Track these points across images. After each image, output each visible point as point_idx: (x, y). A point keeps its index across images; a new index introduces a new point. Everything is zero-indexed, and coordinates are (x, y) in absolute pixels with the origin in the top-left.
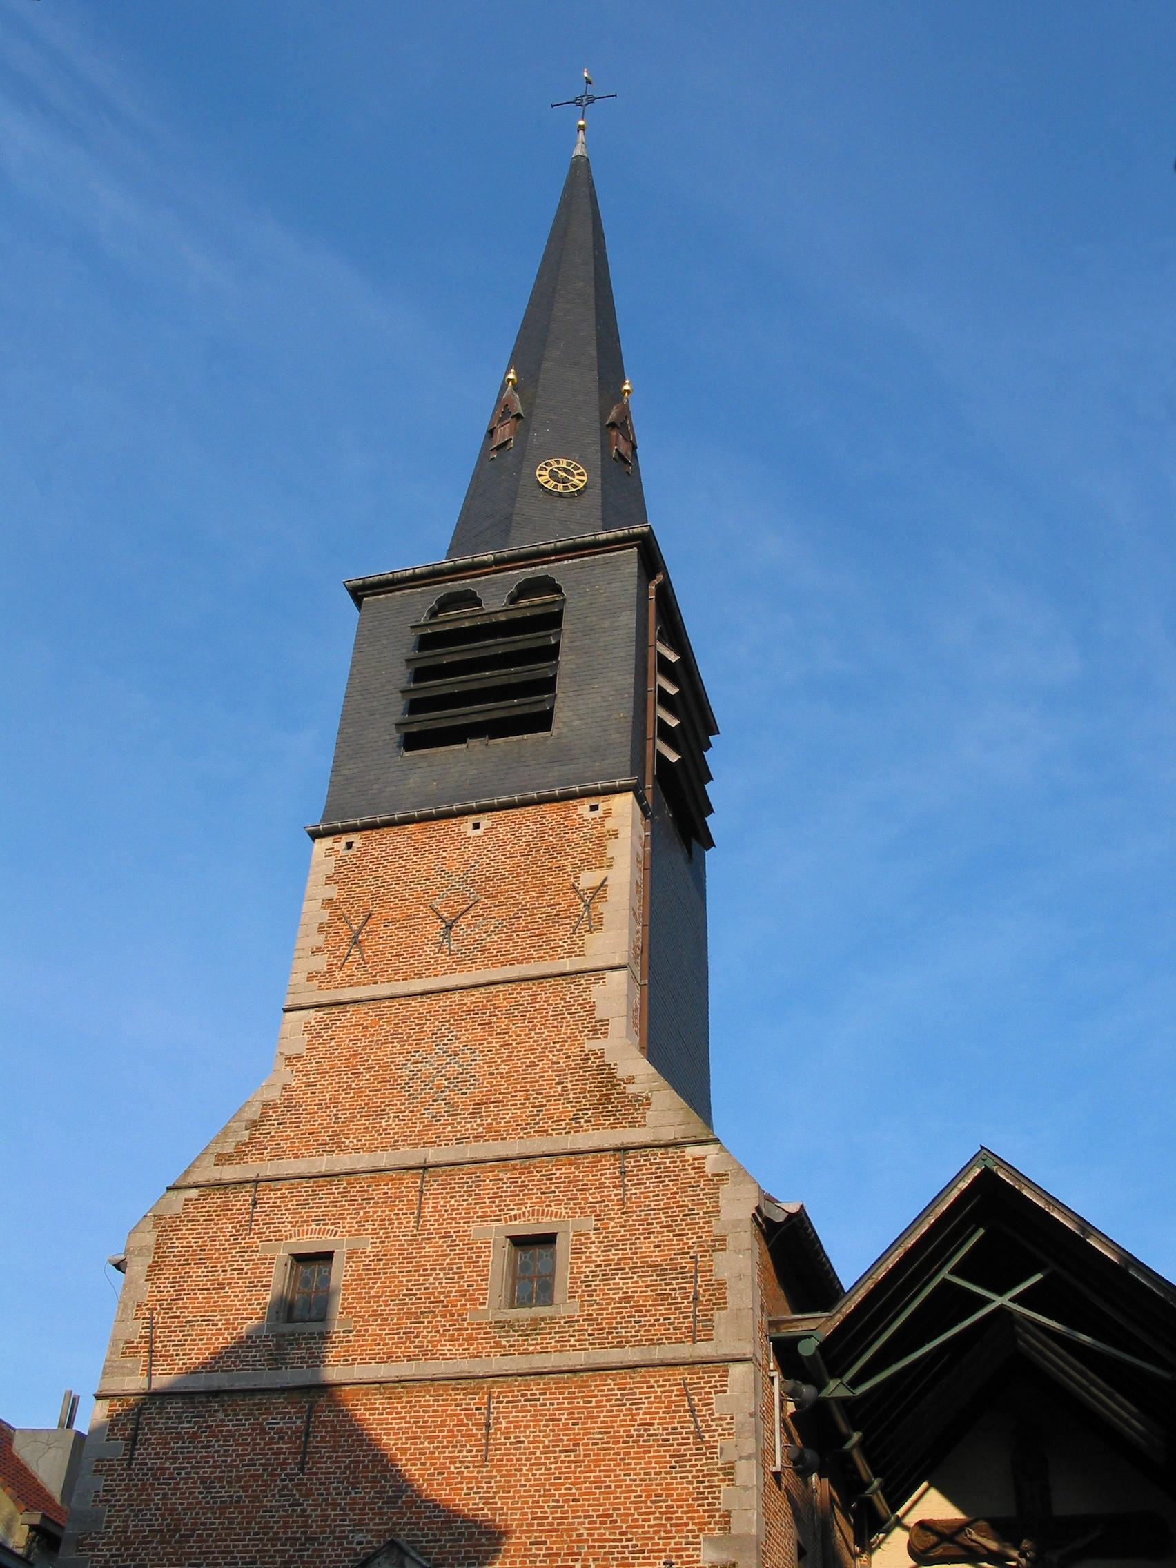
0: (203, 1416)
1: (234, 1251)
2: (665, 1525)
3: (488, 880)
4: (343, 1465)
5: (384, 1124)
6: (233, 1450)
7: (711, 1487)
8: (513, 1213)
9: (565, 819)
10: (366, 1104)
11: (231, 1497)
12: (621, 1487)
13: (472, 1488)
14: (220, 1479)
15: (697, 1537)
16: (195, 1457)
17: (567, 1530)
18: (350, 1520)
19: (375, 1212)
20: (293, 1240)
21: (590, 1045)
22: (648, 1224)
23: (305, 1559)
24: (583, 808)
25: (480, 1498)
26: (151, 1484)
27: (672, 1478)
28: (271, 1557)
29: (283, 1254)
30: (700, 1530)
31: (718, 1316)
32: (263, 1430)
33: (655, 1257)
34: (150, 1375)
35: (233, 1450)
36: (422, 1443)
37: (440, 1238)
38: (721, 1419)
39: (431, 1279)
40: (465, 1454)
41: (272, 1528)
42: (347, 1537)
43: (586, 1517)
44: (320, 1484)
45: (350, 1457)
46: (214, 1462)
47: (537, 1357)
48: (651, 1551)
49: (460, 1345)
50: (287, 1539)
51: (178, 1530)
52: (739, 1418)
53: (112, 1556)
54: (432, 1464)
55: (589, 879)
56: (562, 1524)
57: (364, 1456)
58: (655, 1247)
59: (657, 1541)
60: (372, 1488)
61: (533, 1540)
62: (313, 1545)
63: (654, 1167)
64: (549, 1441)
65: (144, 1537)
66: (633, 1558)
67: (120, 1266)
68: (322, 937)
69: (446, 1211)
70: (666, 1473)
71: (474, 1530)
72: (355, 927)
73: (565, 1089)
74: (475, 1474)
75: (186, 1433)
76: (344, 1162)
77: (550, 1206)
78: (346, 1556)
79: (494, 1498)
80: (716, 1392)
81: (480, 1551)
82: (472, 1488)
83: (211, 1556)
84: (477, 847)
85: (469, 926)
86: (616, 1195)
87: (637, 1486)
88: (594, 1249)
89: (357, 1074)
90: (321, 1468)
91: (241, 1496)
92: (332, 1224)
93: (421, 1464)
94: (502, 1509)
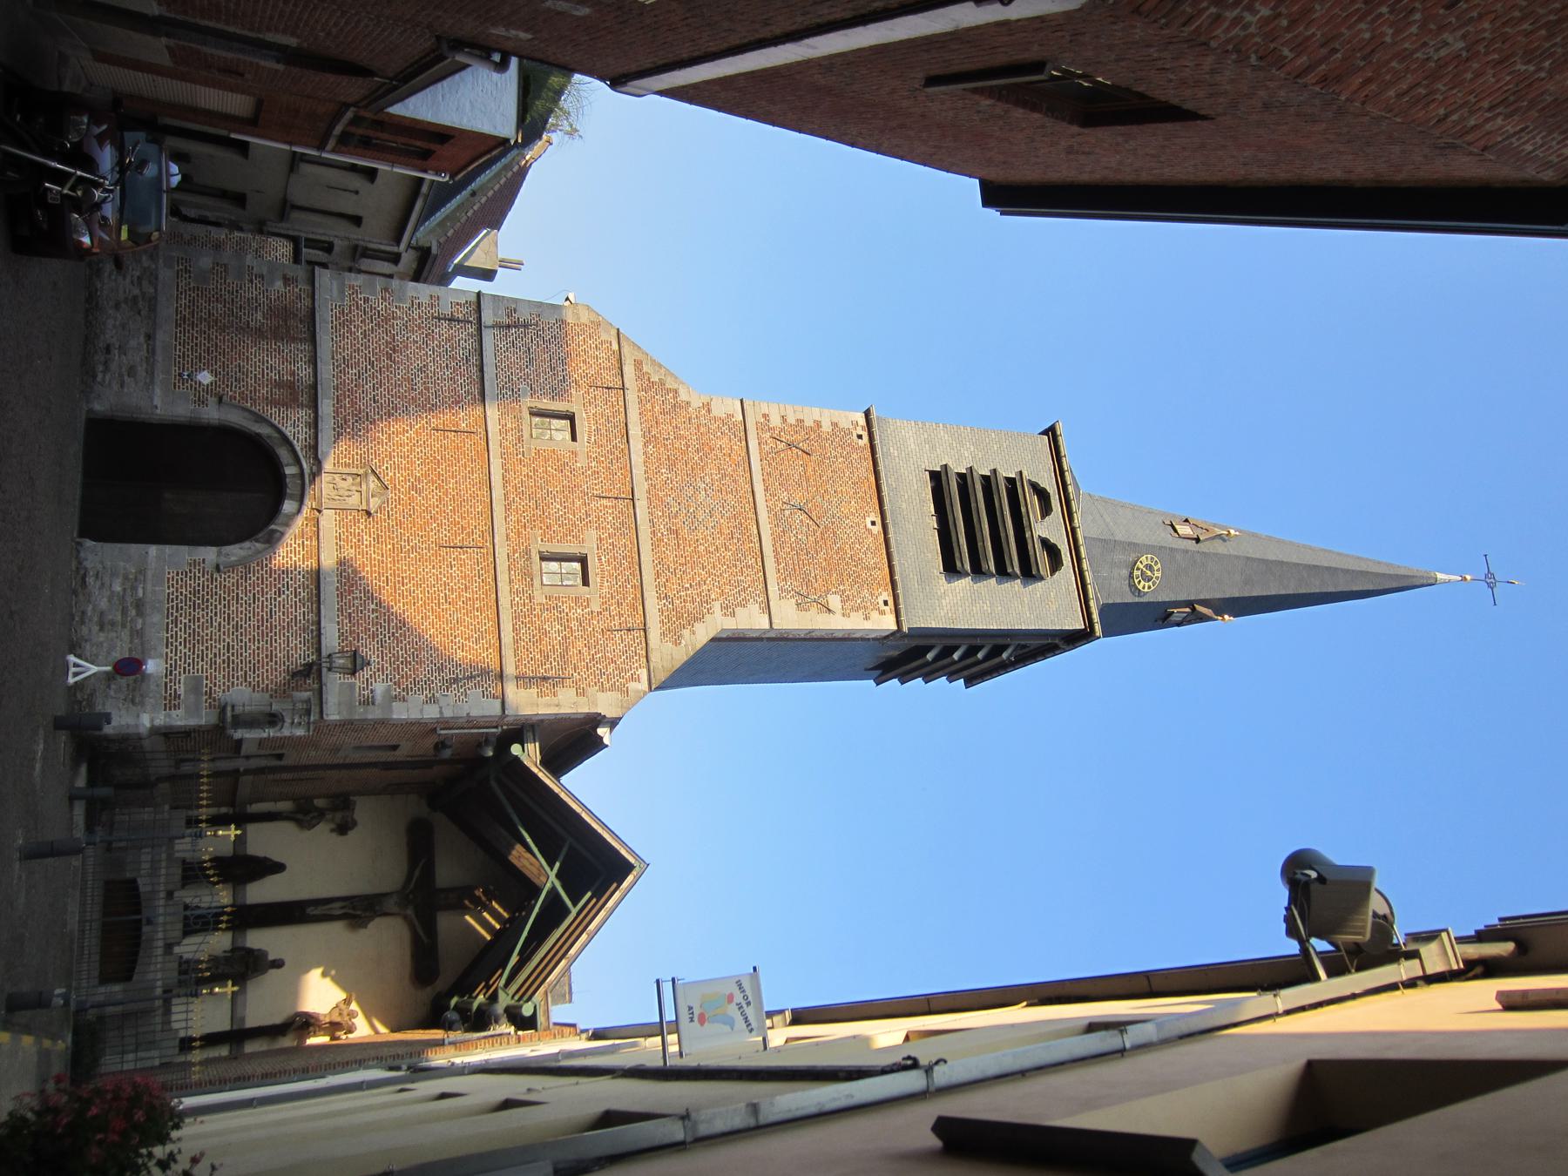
0: (467, 363)
3: (834, 533)
5: (663, 471)
8: (603, 558)
10: (677, 459)
11: (416, 384)
16: (440, 359)
20: (584, 415)
21: (717, 606)
24: (886, 595)
25: (416, 544)
26: (423, 333)
27: (428, 664)
28: (378, 412)
32: (459, 402)
34: (493, 327)
36: (451, 505)
38: (466, 695)
39: (558, 506)
42: (391, 460)
43: (404, 611)
44: (424, 442)
47: (507, 576)
48: (382, 651)
51: (394, 351)
52: (466, 707)
55: (834, 601)
57: (442, 469)
58: (580, 651)
59: (389, 655)
60: (422, 474)
65: (390, 331)
66: (378, 641)
68: (793, 422)
70: (432, 661)
71: (396, 540)
73: (687, 589)
75: (456, 353)
76: (637, 444)
78: (379, 460)
80: (483, 692)
81: (382, 545)
84: (858, 524)
85: (801, 521)
86: (615, 625)
88: (578, 611)
89: (698, 451)
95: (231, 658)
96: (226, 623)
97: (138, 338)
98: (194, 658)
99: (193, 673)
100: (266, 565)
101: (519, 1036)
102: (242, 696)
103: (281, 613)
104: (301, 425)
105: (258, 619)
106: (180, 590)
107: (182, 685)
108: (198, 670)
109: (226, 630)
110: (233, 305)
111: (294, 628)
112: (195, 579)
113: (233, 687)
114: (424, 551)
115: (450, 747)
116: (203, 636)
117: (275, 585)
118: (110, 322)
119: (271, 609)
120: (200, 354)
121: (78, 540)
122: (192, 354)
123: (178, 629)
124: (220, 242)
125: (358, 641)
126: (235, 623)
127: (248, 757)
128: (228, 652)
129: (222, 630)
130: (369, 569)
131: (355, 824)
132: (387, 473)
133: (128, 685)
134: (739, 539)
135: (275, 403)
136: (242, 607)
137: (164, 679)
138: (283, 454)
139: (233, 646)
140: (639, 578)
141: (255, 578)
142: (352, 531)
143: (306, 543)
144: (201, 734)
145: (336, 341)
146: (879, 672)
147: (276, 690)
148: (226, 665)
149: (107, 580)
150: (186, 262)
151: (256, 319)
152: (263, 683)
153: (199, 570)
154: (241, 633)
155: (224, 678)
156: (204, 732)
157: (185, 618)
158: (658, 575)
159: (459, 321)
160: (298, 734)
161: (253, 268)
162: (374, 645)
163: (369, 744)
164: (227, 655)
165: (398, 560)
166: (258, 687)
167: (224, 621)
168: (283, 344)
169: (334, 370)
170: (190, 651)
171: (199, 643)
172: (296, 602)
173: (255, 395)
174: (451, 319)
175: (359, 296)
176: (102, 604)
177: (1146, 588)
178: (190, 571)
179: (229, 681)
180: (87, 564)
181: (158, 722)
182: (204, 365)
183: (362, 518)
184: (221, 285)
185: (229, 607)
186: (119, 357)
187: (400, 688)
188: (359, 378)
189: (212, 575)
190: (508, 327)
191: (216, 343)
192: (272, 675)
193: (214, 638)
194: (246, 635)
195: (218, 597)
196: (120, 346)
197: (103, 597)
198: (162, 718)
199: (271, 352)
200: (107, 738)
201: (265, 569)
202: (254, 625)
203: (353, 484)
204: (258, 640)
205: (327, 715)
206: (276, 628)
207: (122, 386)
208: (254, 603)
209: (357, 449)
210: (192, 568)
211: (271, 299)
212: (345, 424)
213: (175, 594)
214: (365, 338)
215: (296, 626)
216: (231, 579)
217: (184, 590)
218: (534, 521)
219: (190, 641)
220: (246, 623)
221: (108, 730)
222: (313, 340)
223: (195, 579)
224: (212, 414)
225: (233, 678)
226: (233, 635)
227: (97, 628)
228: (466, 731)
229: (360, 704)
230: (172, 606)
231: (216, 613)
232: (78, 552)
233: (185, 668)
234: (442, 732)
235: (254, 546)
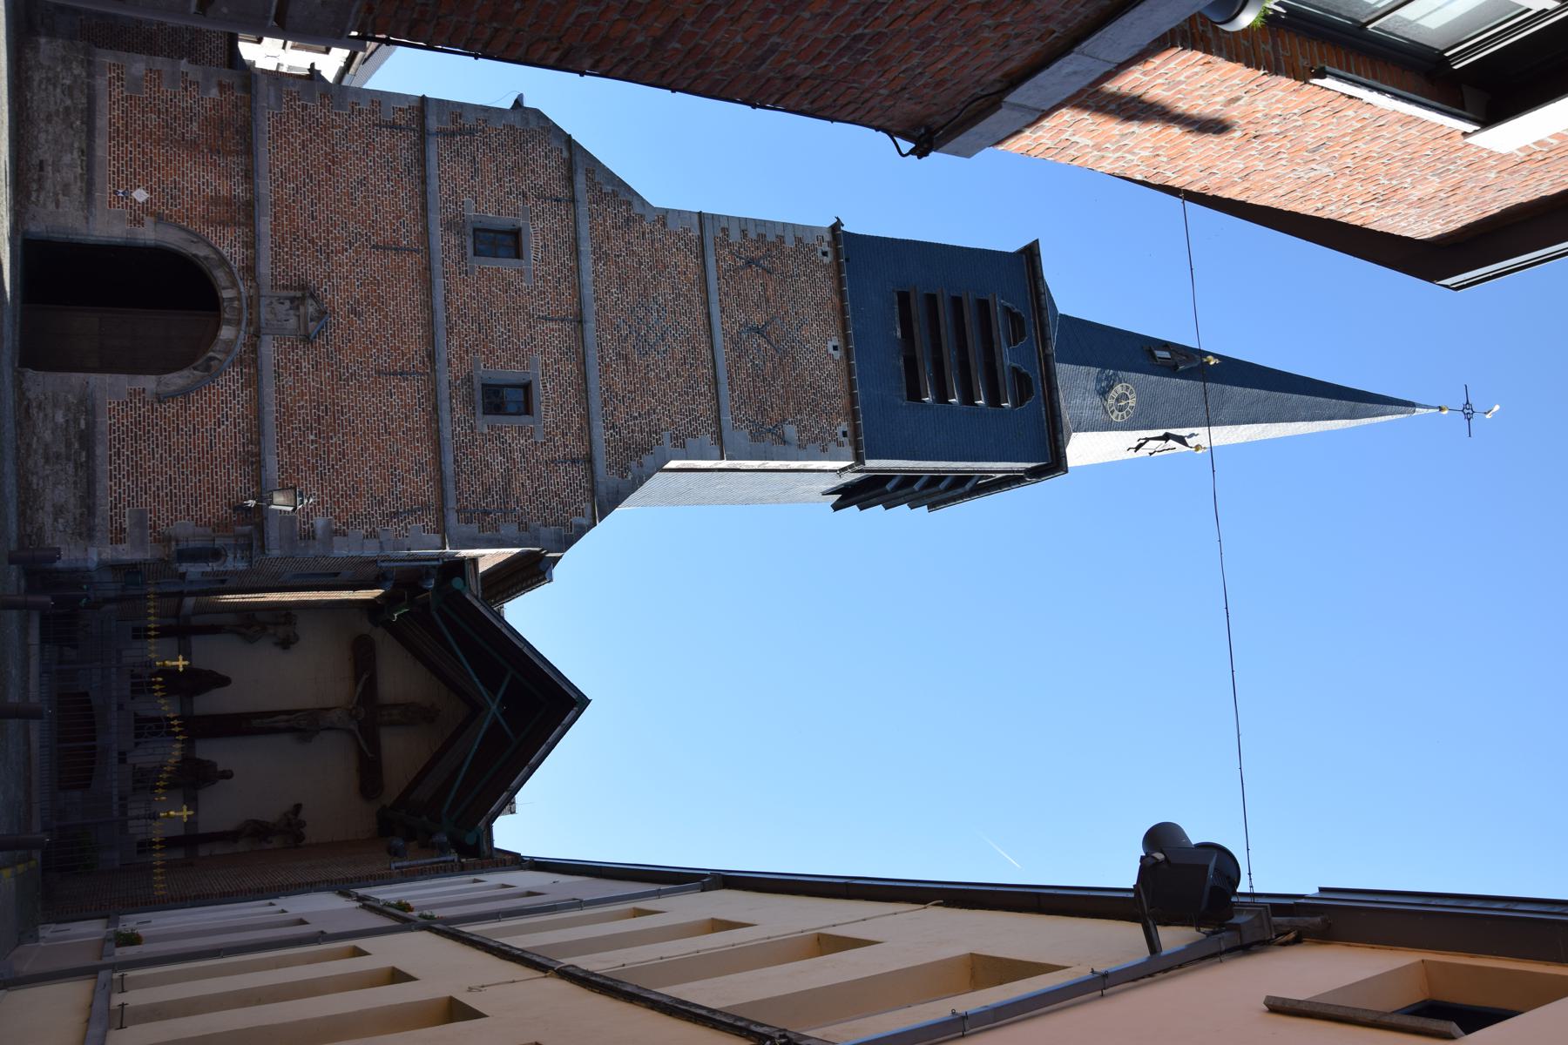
1: (524, 187)
2: (338, 493)
3: (794, 358)
5: (613, 290)
6: (386, 198)
7: (363, 524)
8: (548, 385)
9: (838, 413)
10: (628, 277)
12: (363, 464)
14: (367, 191)
15: (331, 515)
17: (335, 429)
19: (550, 287)
21: (666, 435)
22: (538, 479)
27: (368, 498)
28: (317, 230)
29: (521, 223)
30: (335, 516)
31: (474, 527)
33: (516, 484)
35: (386, 198)
37: (531, 334)
38: (406, 529)
39: (502, 330)
40: (384, 358)
41: (335, 229)
42: (330, 281)
43: (343, 441)
46: (378, 185)
48: (322, 484)
49: (457, 352)
50: (328, 240)
53: (317, 119)
54: (377, 336)
55: (791, 431)
56: (339, 426)
61: (329, 407)
63: (578, 482)
64: (392, 416)
65: (329, 140)
67: (518, 103)
69: (550, 338)
70: (372, 494)
72: (762, 262)
73: (636, 418)
76: (587, 263)
77: (552, 410)
79: (355, 379)
80: (424, 526)
81: (321, 372)
83: (317, 189)
85: (759, 345)
86: (559, 456)
87: (363, 475)
88: (521, 442)
90: (374, 260)
91: (355, 205)
92: (542, 257)
94: (348, 385)
95: (174, 491)
96: (167, 455)
97: (72, 153)
98: (137, 491)
99: (138, 506)
100: (205, 394)
101: (462, 863)
102: (185, 528)
103: (221, 445)
104: (237, 245)
105: (199, 451)
106: (121, 421)
107: (127, 519)
108: (142, 502)
109: (168, 462)
110: (167, 116)
111: (234, 460)
112: (135, 409)
113: (176, 520)
115: (392, 579)
116: (145, 469)
117: (214, 415)
118: (42, 137)
119: (211, 440)
120: (135, 169)
121: (20, 369)
122: (127, 170)
123: (121, 461)
124: (151, 34)
125: (298, 474)
126: (176, 454)
127: (191, 582)
128: (171, 485)
129: (164, 462)
130: (308, 397)
131: (297, 638)
133: (75, 519)
134: (692, 365)
135: (209, 222)
136: (182, 438)
137: (109, 513)
138: (220, 276)
139: (175, 478)
140: (585, 406)
141: (195, 408)
142: (291, 357)
143: (244, 370)
144: (147, 566)
145: (274, 153)
146: (837, 497)
147: (218, 523)
148: (169, 498)
149: (49, 411)
150: (118, 69)
151: (191, 131)
152: (205, 518)
153: (139, 399)
154: (183, 465)
155: (167, 512)
156: (149, 564)
157: (127, 451)
158: (605, 403)
159: (401, 128)
160: (241, 568)
161: (187, 73)
162: (314, 478)
163: (311, 572)
164: (169, 488)
165: (337, 389)
166: (201, 521)
167: (166, 453)
168: (219, 157)
169: (271, 185)
170: (133, 484)
171: (141, 476)
172: (235, 433)
173: (192, 214)
174: (393, 126)
175: (297, 103)
176: (47, 436)
177: (1119, 417)
178: (131, 400)
179: (172, 515)
180: (31, 395)
181: (104, 556)
182: (139, 182)
184: (154, 94)
185: (170, 438)
186: (53, 173)
187: (340, 523)
188: (297, 193)
189: (152, 405)
190: (453, 134)
191: (151, 158)
192: (213, 509)
193: (156, 470)
194: (187, 468)
195: (159, 428)
196: (53, 162)
197: (47, 429)
198: (110, 552)
199: (207, 166)
200: (58, 571)
201: (204, 398)
202: (195, 457)
203: (291, 309)
204: (200, 472)
205: (269, 550)
206: (216, 460)
207: (57, 206)
208: (194, 434)
209: (295, 269)
210: (133, 398)
211: (206, 108)
212: (283, 242)
213: (117, 425)
214: (304, 149)
215: (236, 458)
216: (171, 409)
217: (125, 421)
218: (477, 345)
219: (133, 473)
220: (186, 455)
221: (59, 564)
222: (249, 150)
223: (135, 409)
224: (148, 234)
225: (176, 512)
226: (174, 467)
227: (43, 461)
228: (406, 563)
229: (301, 539)
230: (115, 437)
231: (157, 444)
232: (21, 382)
233: (129, 501)
234: (383, 564)
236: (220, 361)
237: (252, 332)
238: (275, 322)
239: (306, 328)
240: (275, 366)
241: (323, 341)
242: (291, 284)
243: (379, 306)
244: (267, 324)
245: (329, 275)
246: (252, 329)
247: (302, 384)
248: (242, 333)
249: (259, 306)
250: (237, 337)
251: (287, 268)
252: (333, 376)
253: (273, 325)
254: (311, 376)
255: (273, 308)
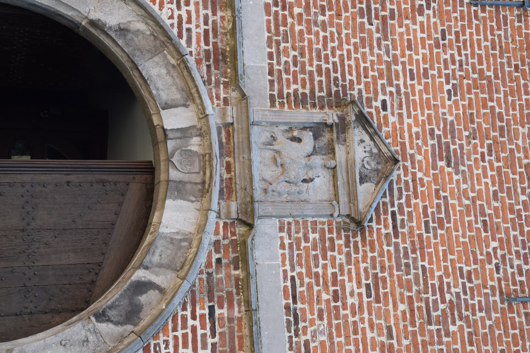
4: (485, 66)
13: (470, 280)
18: (413, 86)
23: (359, 20)
40: (516, 262)
42: (391, 84)
44: (457, 33)
45: (496, 77)
57: (499, 99)
60: (458, 116)
62: (378, 31)
71: (415, 288)
74: (490, 283)
78: (367, 84)
82: (470, 280)
90: (478, 34)
93: (495, 193)
94: (447, 335)
114: (479, 314)
132: (385, 117)
142: (320, 270)
143: (218, 312)
183: (339, 237)
209: (319, 58)
235: (95, 332)
236: (162, 291)
237: (234, 215)
238: (282, 187)
239: (352, 196)
240: (286, 297)
241: (386, 227)
242: (312, 91)
243: (495, 139)
244: (265, 191)
245: (389, 69)
246: (234, 206)
247: (347, 337)
248: (212, 216)
249: (250, 149)
250: (201, 228)
251: (302, 55)
252: (412, 311)
253: (280, 194)
254: (366, 315)
255: (278, 152)
